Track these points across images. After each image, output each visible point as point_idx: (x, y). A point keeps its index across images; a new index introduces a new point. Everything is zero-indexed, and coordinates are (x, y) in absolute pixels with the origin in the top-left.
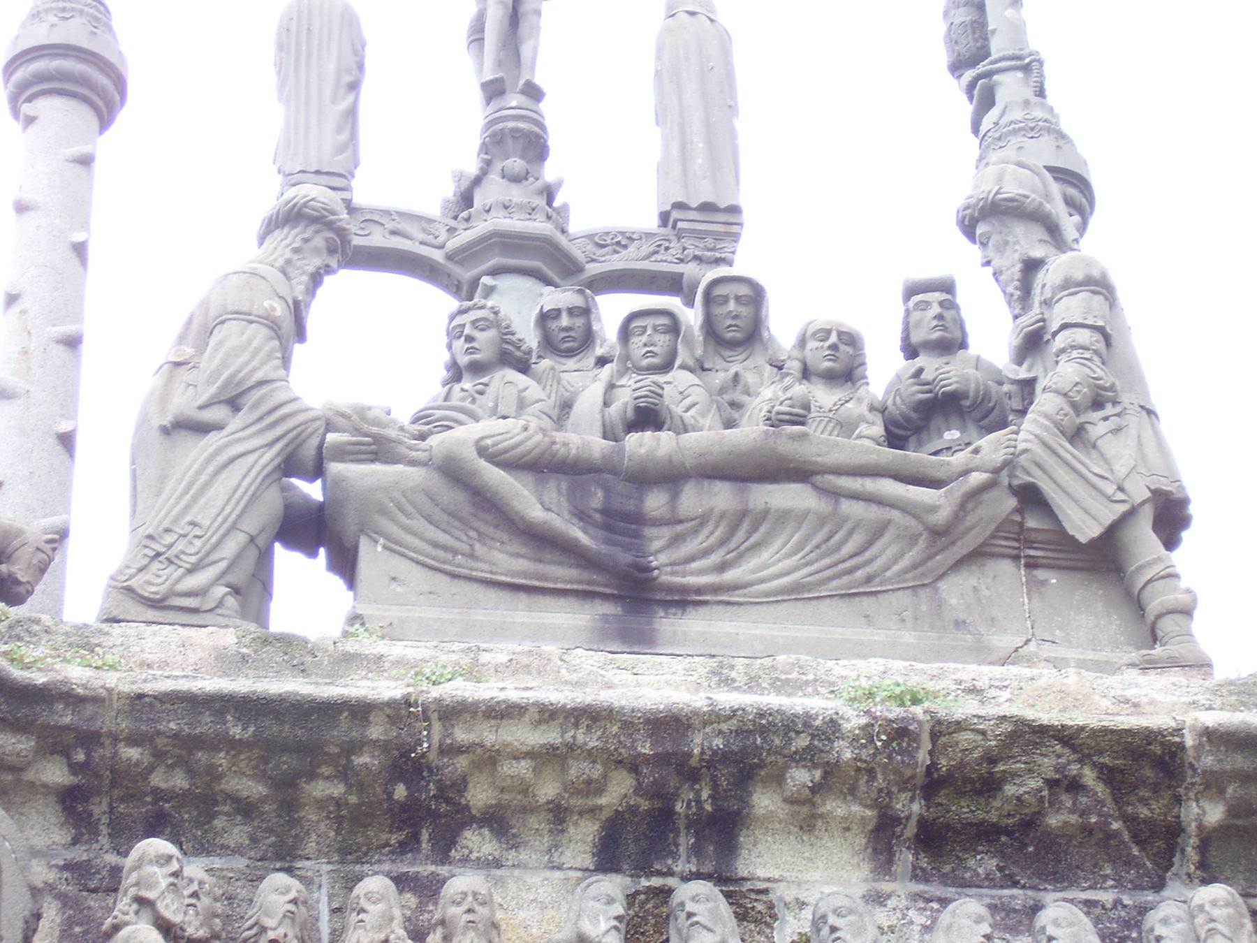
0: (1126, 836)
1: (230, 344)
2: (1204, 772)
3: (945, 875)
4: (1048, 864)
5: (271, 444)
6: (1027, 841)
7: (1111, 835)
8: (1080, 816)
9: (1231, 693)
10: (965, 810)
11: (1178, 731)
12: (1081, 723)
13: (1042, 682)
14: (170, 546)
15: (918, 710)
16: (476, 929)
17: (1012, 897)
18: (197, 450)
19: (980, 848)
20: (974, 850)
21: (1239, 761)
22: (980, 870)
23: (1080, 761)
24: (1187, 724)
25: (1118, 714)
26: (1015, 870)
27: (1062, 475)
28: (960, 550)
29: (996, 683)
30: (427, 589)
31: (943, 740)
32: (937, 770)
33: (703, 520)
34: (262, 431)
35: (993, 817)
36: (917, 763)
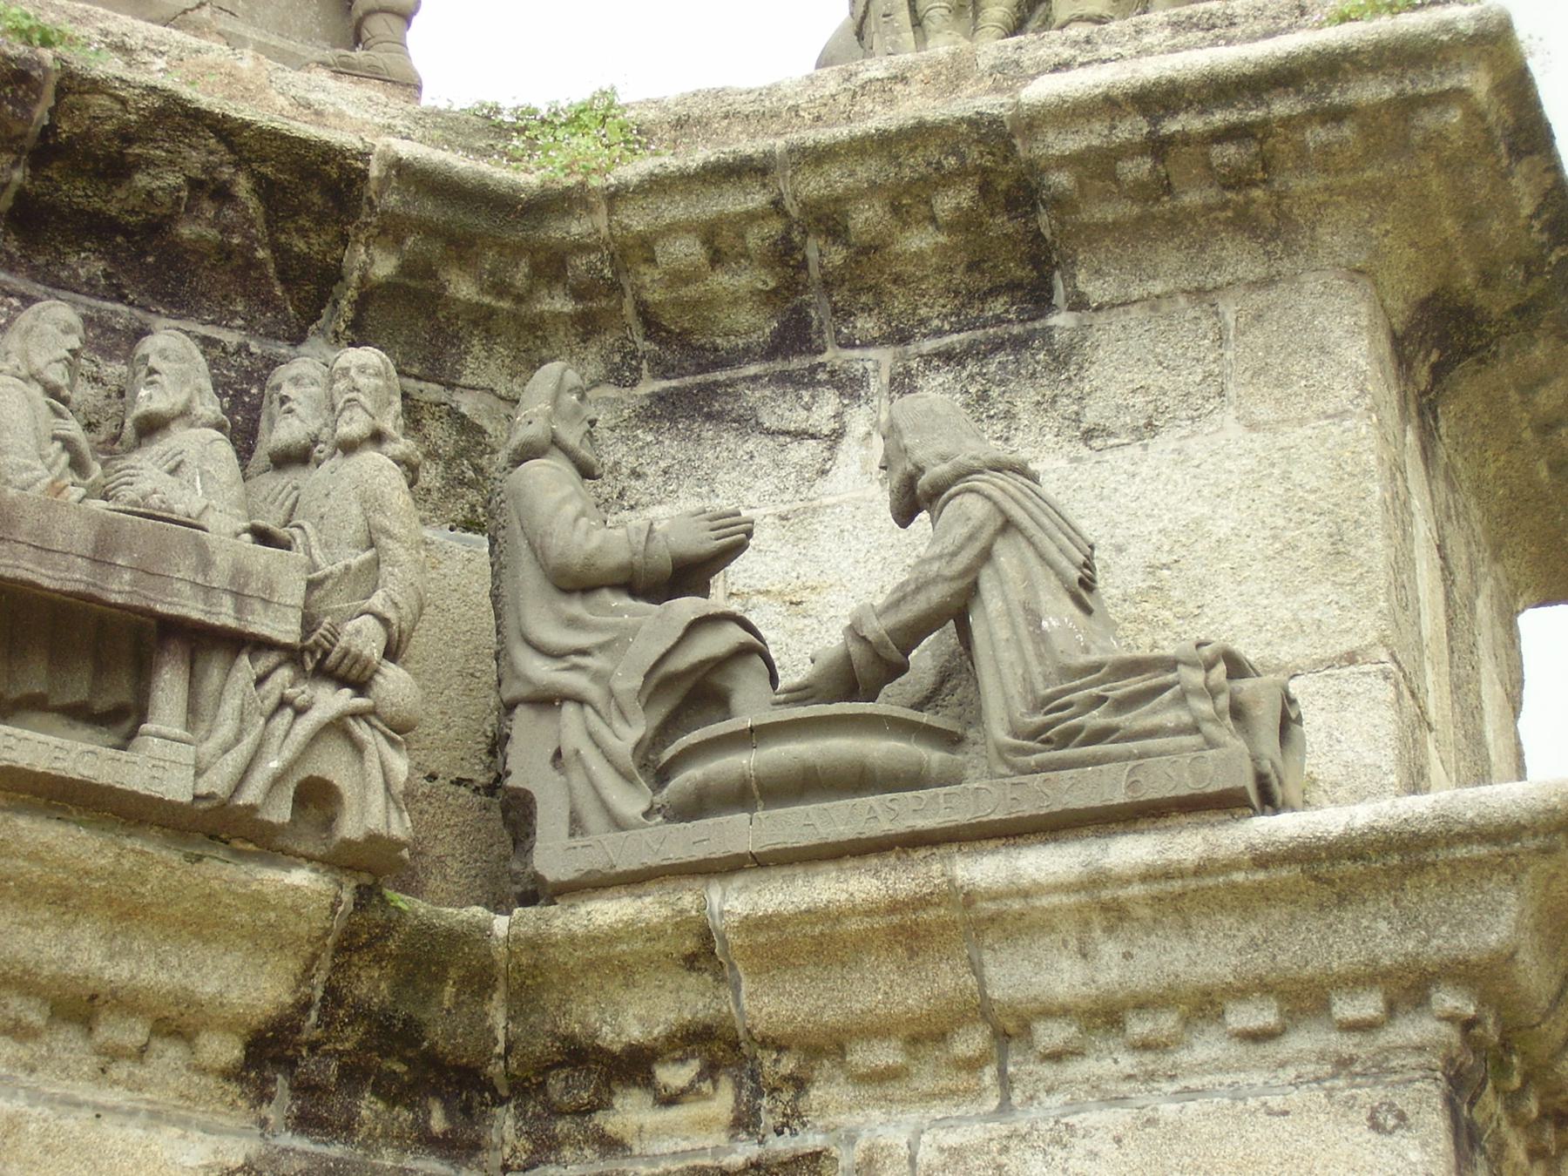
0: (271, 271)
2: (384, 213)
3: (35, 268)
4: (168, 282)
6: (149, 249)
7: (252, 264)
8: (221, 233)
9: (435, 126)
10: (79, 193)
11: (364, 155)
12: (248, 118)
13: (209, 58)
15: (47, 55)
17: (115, 313)
19: (87, 244)
20: (80, 245)
21: (429, 209)
22: (81, 271)
23: (236, 165)
24: (377, 149)
25: (294, 119)
26: (125, 280)
29: (152, 46)
31: (71, 98)
32: (55, 134)
35: (113, 209)
36: (32, 119)
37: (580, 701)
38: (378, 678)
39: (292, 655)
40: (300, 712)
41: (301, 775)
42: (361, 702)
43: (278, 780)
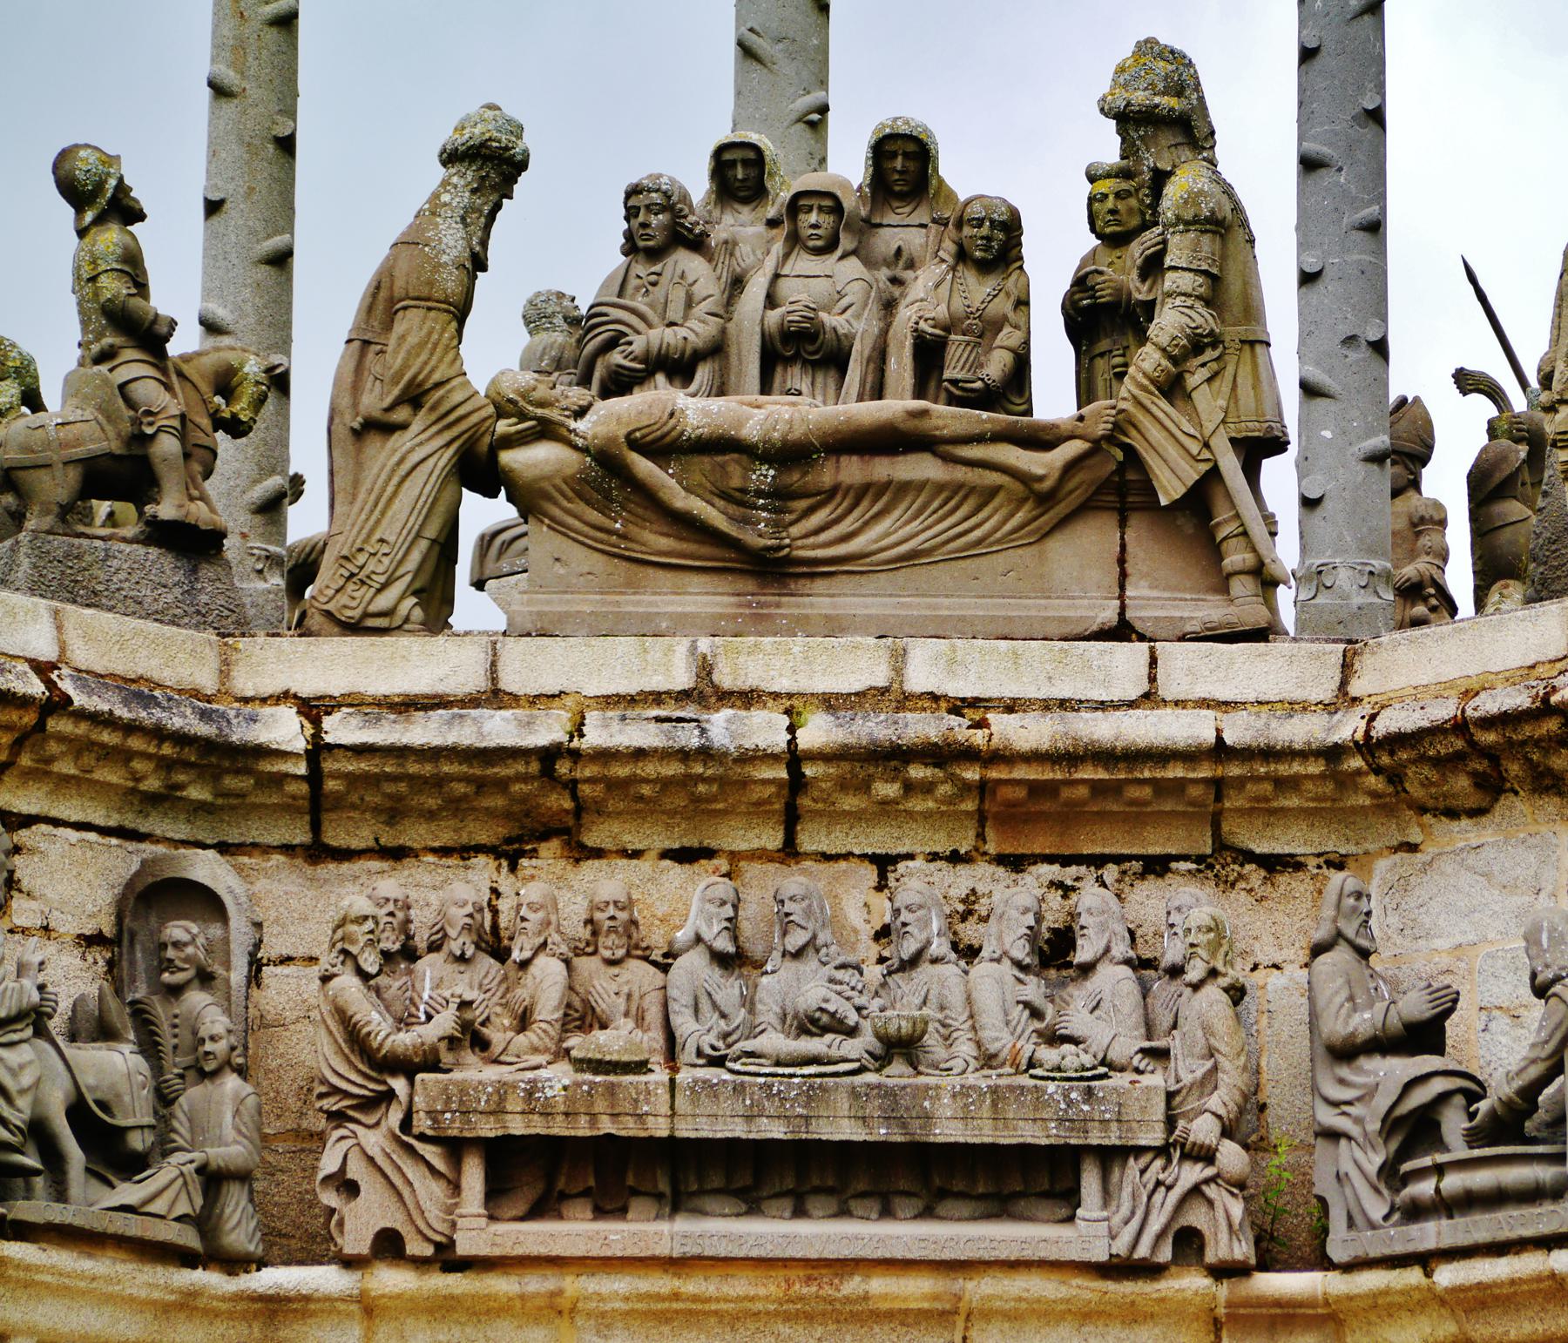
1: (412, 340)
5: (448, 445)
14: (362, 568)
16: (616, 932)
18: (383, 454)
27: (1155, 433)
28: (1061, 509)
30: (586, 569)
33: (832, 493)
34: (439, 432)
37: (1350, 1138)
39: (1163, 1151)
40: (1169, 1188)
41: (1176, 1227)
42: (1210, 1171)
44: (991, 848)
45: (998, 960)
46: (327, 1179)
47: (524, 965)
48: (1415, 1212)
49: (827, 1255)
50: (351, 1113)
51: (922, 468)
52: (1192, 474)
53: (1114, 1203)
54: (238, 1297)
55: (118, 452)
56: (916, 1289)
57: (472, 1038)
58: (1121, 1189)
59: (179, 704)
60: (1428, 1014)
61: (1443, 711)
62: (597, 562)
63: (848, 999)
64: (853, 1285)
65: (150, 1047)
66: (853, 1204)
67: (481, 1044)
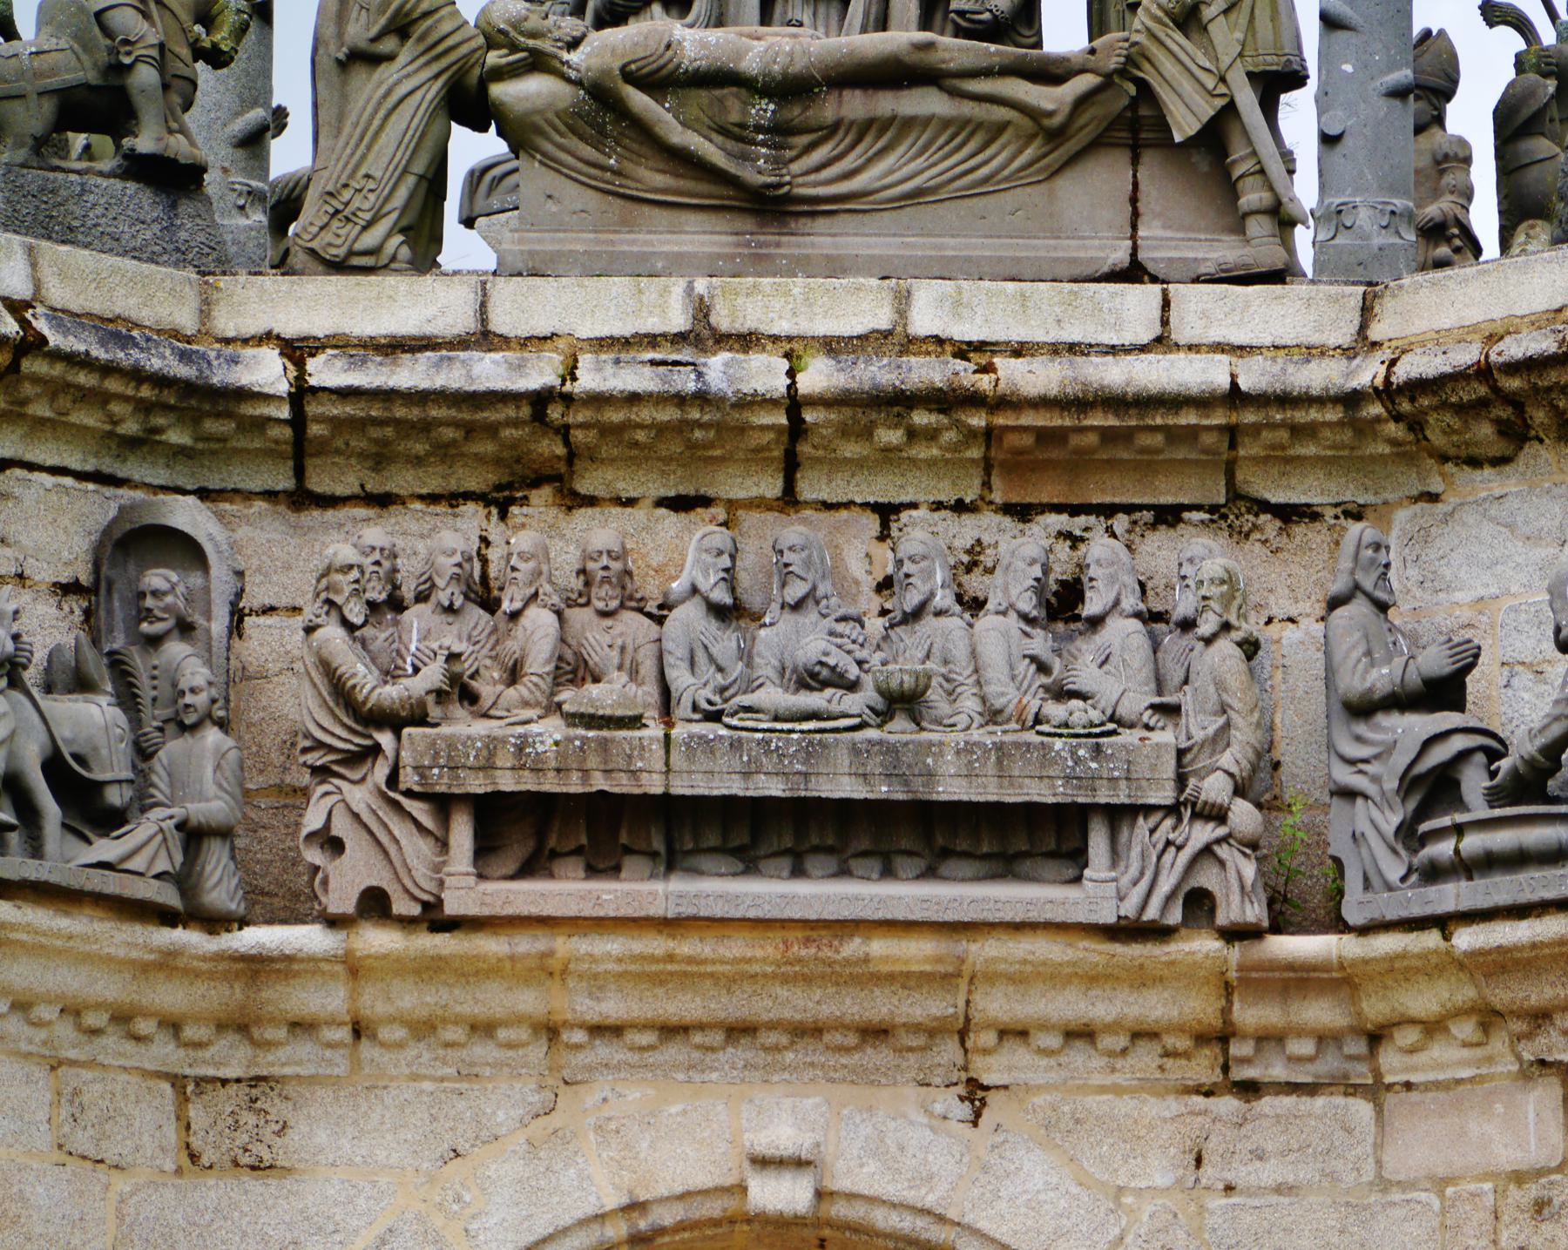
5: (436, 76)
14: (347, 204)
16: (610, 583)
18: (369, 86)
27: (1168, 66)
28: (1071, 146)
30: (580, 207)
33: (833, 129)
37: (1366, 797)
38: (1230, 814)
39: (1173, 810)
40: (1179, 848)
41: (1186, 888)
42: (1221, 831)
43: (1170, 898)
44: (998, 497)
45: (1004, 613)
46: (311, 836)
47: (515, 616)
48: (1433, 873)
49: (826, 916)
50: (335, 768)
51: (927, 103)
52: (1207, 109)
53: (1122, 864)
54: (219, 957)
55: (94, 82)
56: (917, 951)
57: (460, 691)
58: (1129, 848)
59: (157, 344)
60: (1448, 669)
61: (1466, 356)
62: (591, 199)
63: (849, 652)
64: (853, 947)
65: (128, 699)
66: (854, 864)
67: (469, 697)
